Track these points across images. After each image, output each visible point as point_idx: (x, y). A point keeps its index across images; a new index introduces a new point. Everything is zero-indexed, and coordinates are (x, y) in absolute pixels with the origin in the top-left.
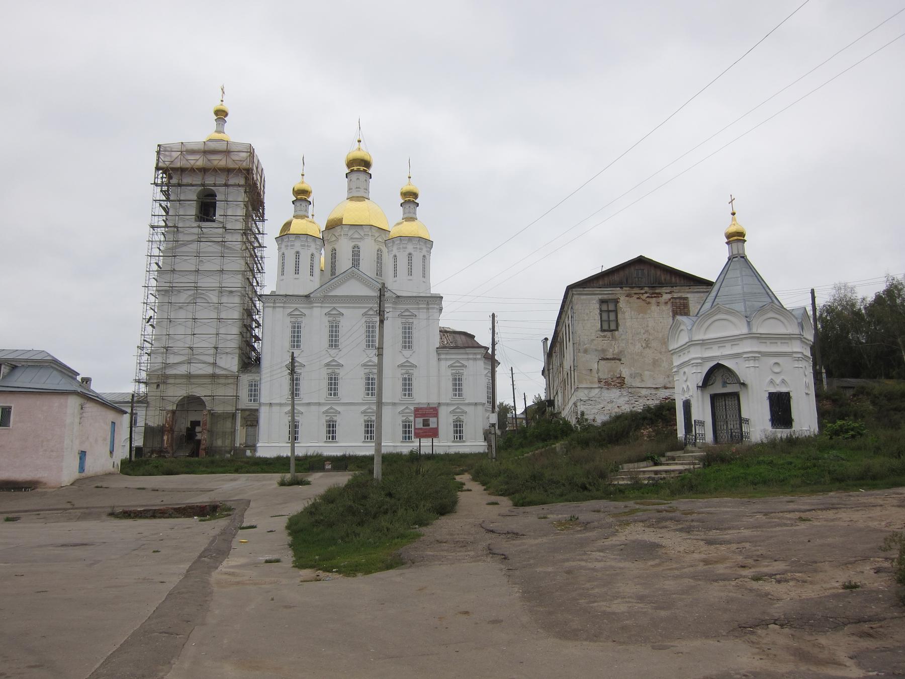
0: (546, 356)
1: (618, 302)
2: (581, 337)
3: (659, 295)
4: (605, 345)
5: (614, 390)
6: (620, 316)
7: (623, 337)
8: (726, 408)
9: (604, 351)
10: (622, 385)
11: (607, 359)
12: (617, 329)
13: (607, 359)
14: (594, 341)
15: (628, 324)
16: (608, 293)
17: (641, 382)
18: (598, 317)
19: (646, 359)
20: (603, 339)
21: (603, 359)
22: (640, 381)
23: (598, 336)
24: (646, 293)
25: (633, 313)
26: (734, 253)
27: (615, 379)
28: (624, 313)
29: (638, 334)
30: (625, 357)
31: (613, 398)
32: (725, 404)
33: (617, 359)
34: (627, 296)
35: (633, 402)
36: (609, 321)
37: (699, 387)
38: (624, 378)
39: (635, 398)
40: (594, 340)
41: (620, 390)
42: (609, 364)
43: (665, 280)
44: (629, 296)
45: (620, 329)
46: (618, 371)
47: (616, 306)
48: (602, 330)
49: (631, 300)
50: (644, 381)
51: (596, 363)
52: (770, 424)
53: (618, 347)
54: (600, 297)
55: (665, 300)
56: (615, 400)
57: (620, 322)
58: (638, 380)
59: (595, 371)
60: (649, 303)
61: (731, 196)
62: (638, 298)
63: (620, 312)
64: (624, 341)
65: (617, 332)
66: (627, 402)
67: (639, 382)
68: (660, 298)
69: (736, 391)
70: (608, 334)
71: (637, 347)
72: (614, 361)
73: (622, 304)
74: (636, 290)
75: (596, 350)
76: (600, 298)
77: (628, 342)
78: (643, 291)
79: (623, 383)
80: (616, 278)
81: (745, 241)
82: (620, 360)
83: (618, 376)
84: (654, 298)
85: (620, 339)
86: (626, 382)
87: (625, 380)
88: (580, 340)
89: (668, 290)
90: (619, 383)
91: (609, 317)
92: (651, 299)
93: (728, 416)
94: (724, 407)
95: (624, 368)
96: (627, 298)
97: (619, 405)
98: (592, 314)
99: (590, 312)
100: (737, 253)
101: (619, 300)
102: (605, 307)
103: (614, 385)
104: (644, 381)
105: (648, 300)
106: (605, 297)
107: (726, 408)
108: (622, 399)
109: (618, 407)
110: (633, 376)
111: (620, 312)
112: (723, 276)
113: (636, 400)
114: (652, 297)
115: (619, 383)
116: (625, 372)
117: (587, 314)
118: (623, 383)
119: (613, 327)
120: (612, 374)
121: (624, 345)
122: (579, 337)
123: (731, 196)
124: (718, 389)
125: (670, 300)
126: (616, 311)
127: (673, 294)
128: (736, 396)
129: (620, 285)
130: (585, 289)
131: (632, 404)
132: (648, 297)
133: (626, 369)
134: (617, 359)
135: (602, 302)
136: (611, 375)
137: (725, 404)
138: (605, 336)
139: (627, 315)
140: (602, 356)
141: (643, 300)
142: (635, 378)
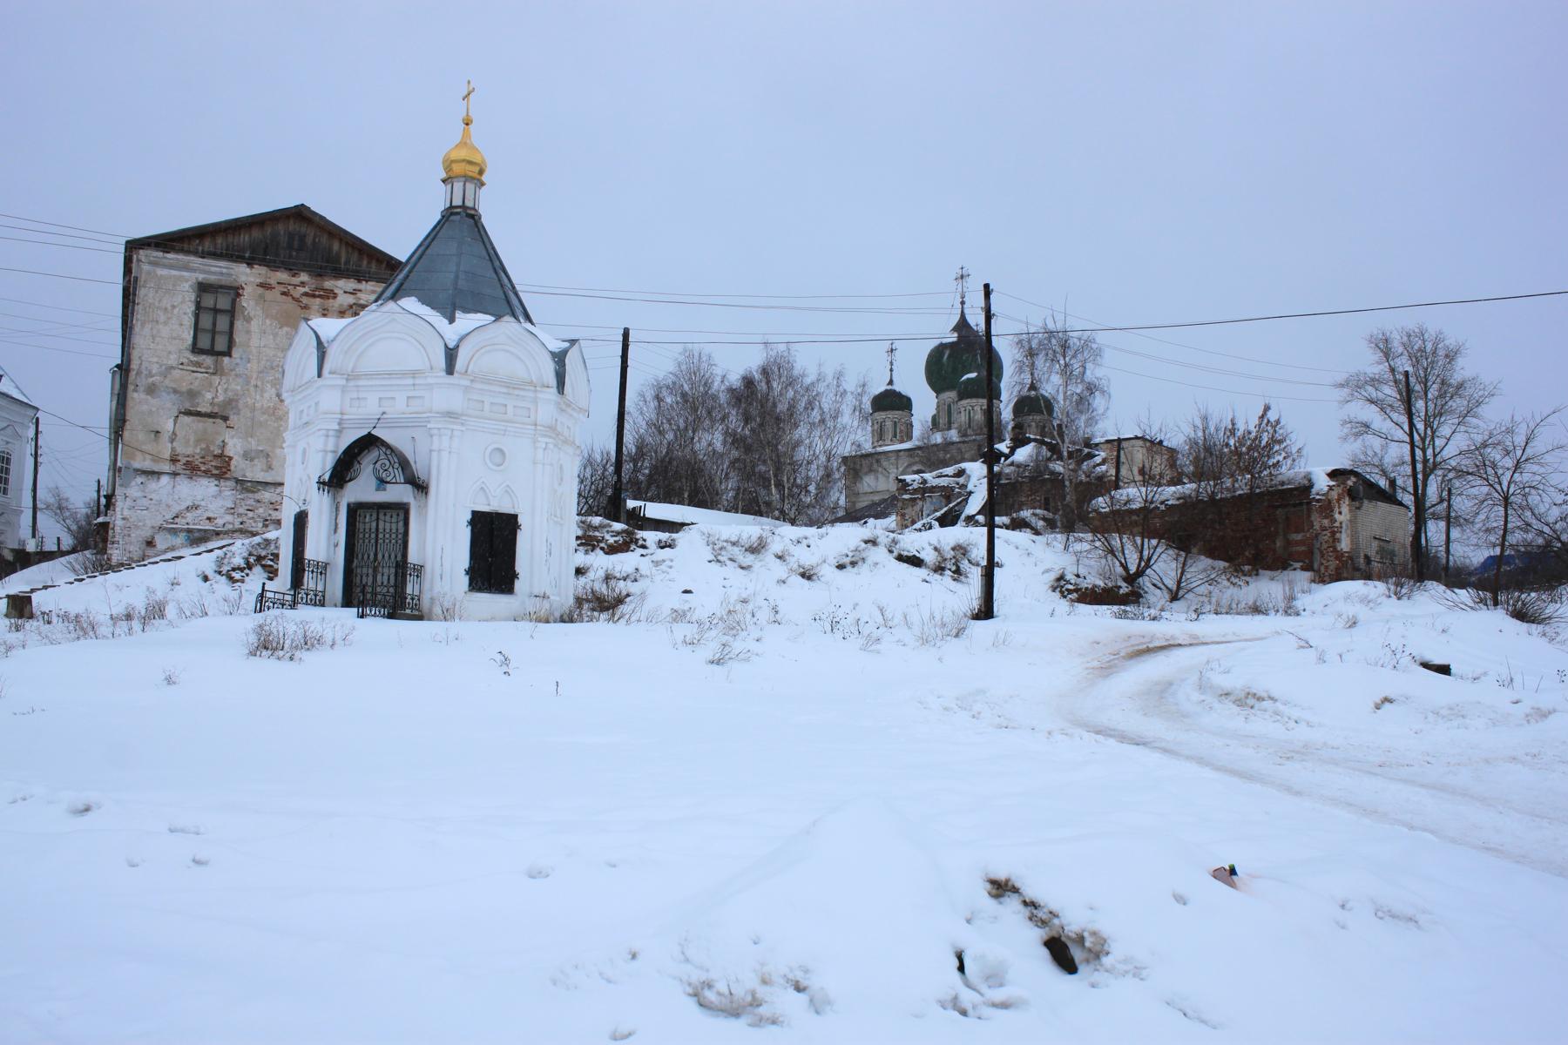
0: (115, 402)
1: (238, 295)
2: (143, 358)
3: (329, 294)
4: (196, 383)
5: (204, 481)
6: (238, 324)
7: (239, 370)
8: (377, 536)
9: (192, 394)
10: (226, 473)
11: (199, 414)
12: (228, 354)
13: (199, 414)
14: (172, 371)
15: (255, 342)
16: (217, 270)
17: (267, 471)
18: (189, 320)
19: (282, 423)
20: (195, 369)
21: (189, 413)
22: (265, 467)
23: (185, 361)
24: (303, 284)
25: (268, 322)
26: (454, 204)
27: (210, 458)
28: (248, 320)
29: (272, 368)
30: (239, 414)
31: (199, 497)
32: (377, 529)
33: (219, 416)
34: (261, 285)
35: (241, 510)
36: (214, 332)
37: (324, 483)
38: (231, 458)
39: (248, 503)
40: (172, 368)
41: (216, 482)
42: (201, 424)
43: (347, 262)
44: (265, 286)
45: (236, 353)
46: (219, 442)
47: (234, 302)
48: (195, 349)
49: (269, 294)
50: (272, 469)
51: (172, 420)
52: (466, 580)
53: (226, 390)
54: (201, 277)
55: (341, 305)
56: (203, 503)
57: (238, 338)
58: (259, 464)
59: (165, 437)
60: (306, 307)
61: (469, 82)
62: (284, 294)
63: (241, 318)
64: (240, 380)
65: (226, 359)
66: (231, 510)
67: (262, 470)
68: (331, 301)
69: (405, 500)
70: (208, 360)
71: (266, 395)
72: (211, 420)
73: (247, 302)
74: (282, 276)
75: (175, 391)
76: (200, 279)
77: (248, 383)
78: (296, 280)
79: (225, 468)
80: (244, 238)
81: (483, 184)
82: (225, 419)
83: (217, 452)
84: (318, 299)
85: (234, 372)
86: (232, 468)
87: (233, 463)
88: (141, 364)
89: (350, 284)
90: (217, 468)
91: (214, 324)
92: (312, 300)
93: (380, 556)
94: (373, 536)
95: (232, 437)
96: (260, 290)
97: (211, 515)
98: (176, 311)
99: (174, 307)
100: (460, 203)
101: (240, 291)
102: (208, 301)
103: (204, 471)
104: (272, 469)
105: (305, 300)
106: (212, 278)
107: (377, 536)
108: (220, 502)
109: (209, 519)
110: (248, 456)
111: (241, 318)
112: (422, 248)
113: (250, 508)
114: (314, 296)
115: (217, 468)
116: (235, 447)
117: (166, 309)
118: (225, 468)
119: (221, 345)
120: (204, 446)
121: (239, 388)
122: (140, 358)
123: (469, 82)
124: (362, 489)
125: (351, 307)
126: (232, 313)
127: (359, 295)
128: (402, 509)
129: (251, 258)
130: (169, 256)
131: (240, 515)
132: (306, 294)
133: (235, 440)
134: (219, 416)
135: (203, 288)
136: (201, 449)
137: (377, 529)
138: (198, 364)
139: (255, 326)
140: (188, 405)
141: (296, 300)
142: (252, 460)
